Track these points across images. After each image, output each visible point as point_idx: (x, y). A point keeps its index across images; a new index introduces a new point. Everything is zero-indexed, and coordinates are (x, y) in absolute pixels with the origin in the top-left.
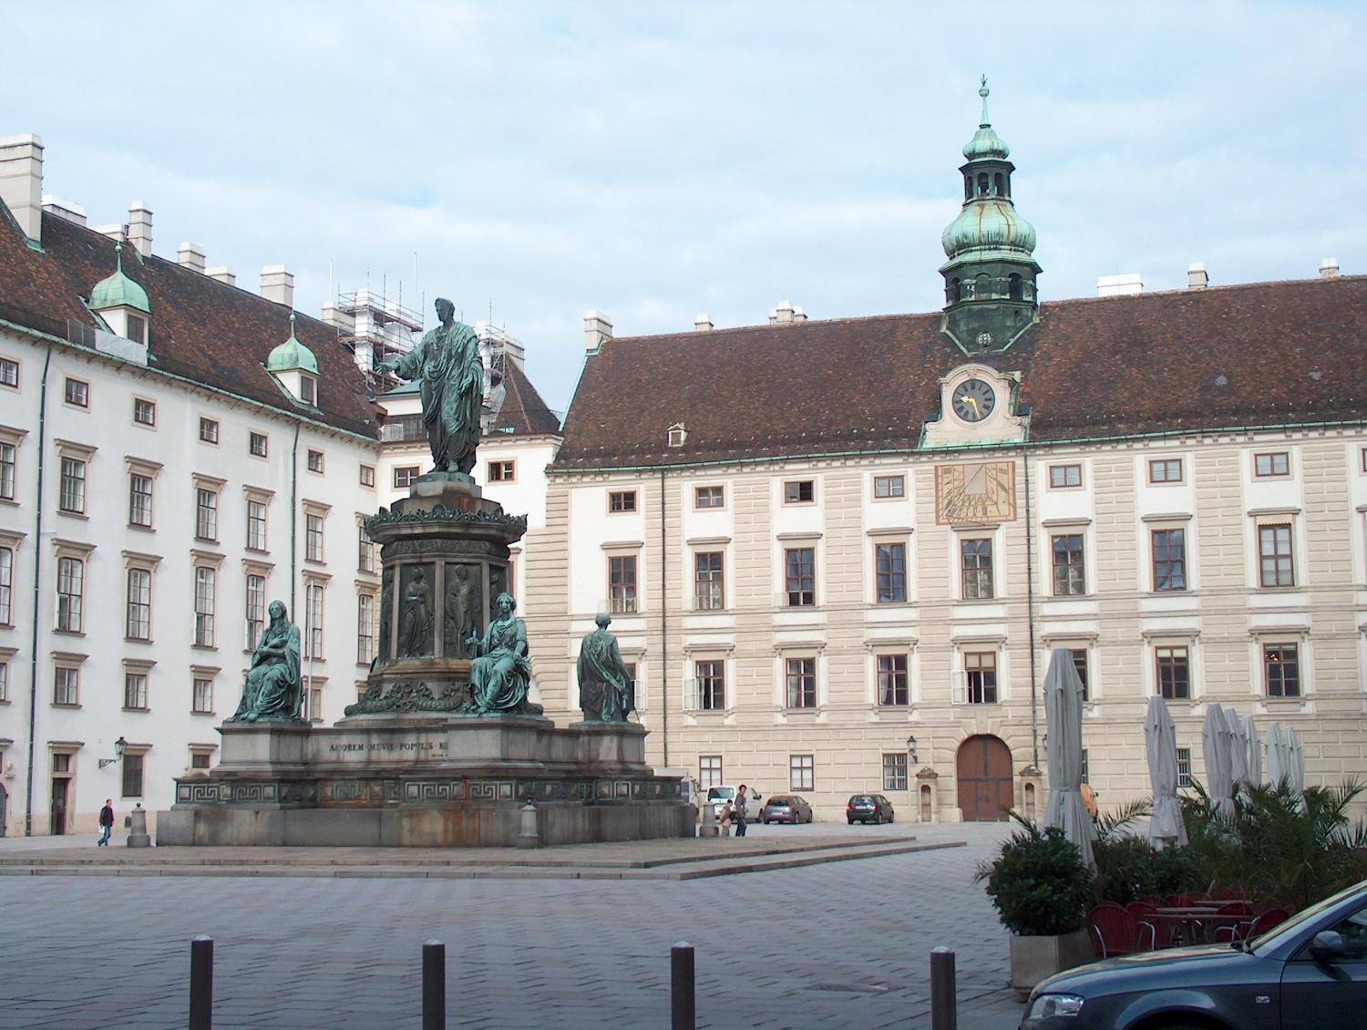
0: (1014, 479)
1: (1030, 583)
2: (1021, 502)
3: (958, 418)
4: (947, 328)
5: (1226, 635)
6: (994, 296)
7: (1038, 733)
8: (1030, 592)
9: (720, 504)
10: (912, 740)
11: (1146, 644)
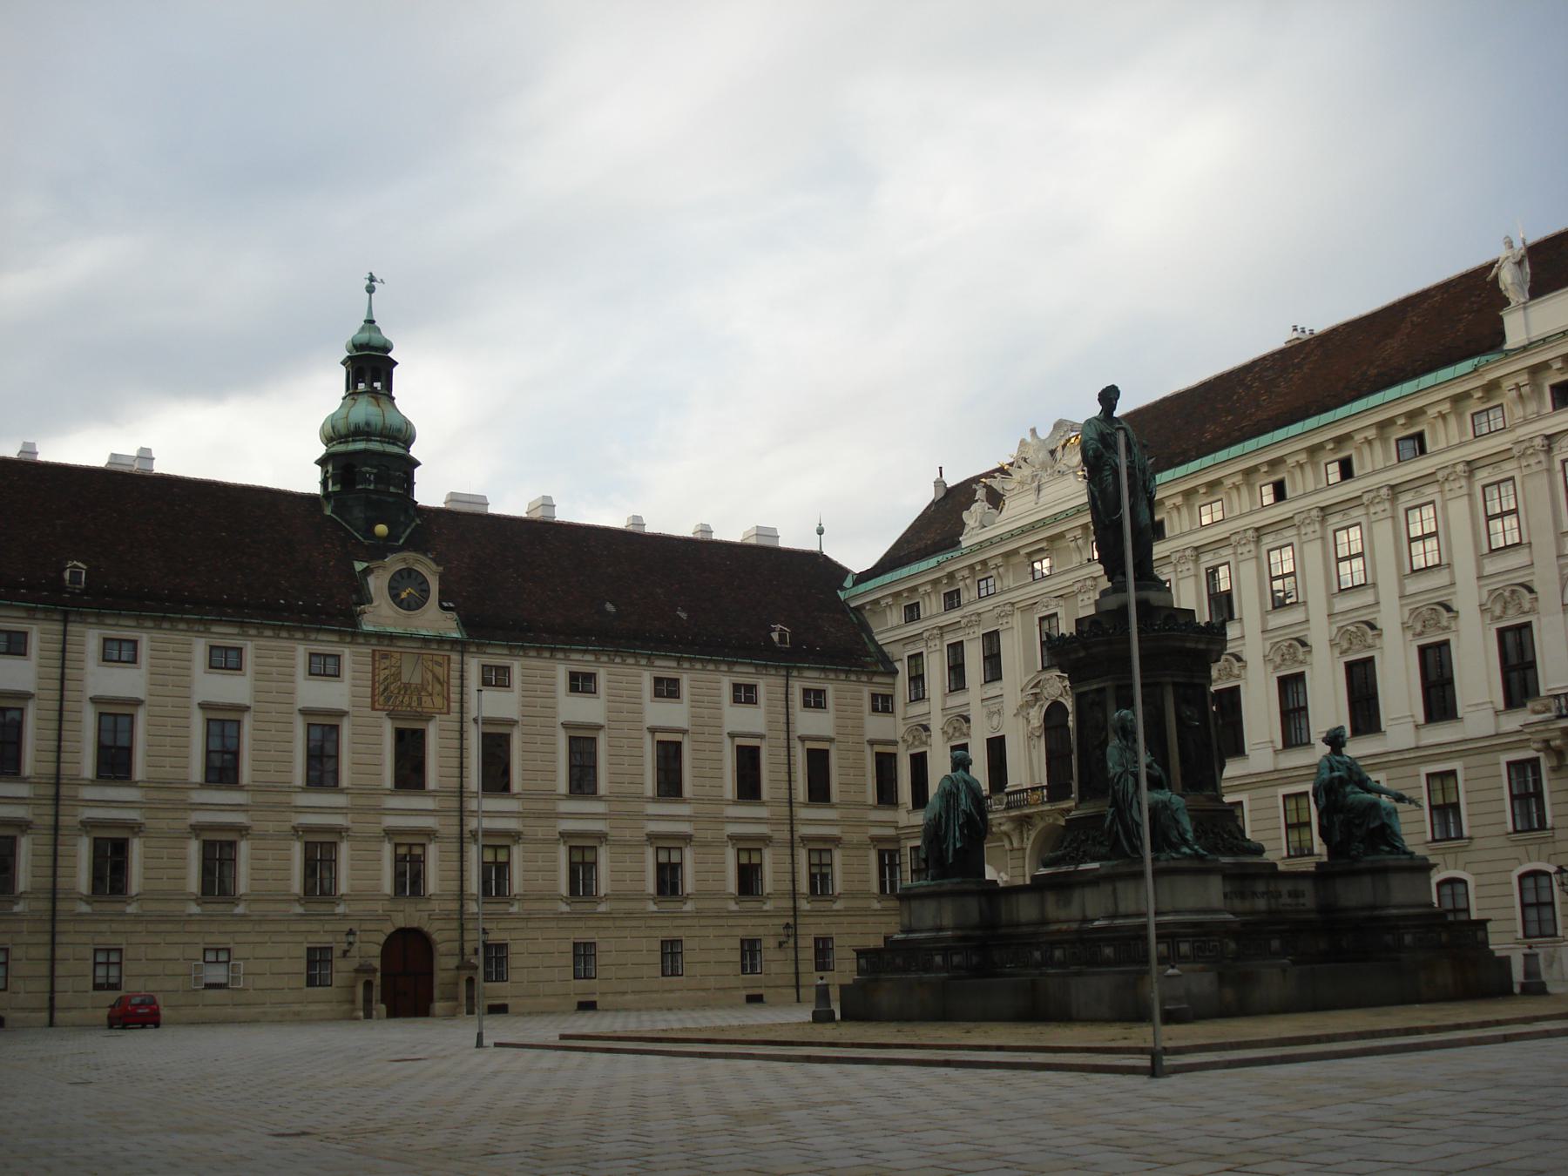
0: (448, 676)
1: (461, 777)
2: (455, 697)
3: (395, 606)
4: (332, 512)
5: (628, 838)
6: (392, 489)
7: (465, 926)
8: (462, 786)
9: (134, 660)
10: (351, 932)
11: (562, 844)
